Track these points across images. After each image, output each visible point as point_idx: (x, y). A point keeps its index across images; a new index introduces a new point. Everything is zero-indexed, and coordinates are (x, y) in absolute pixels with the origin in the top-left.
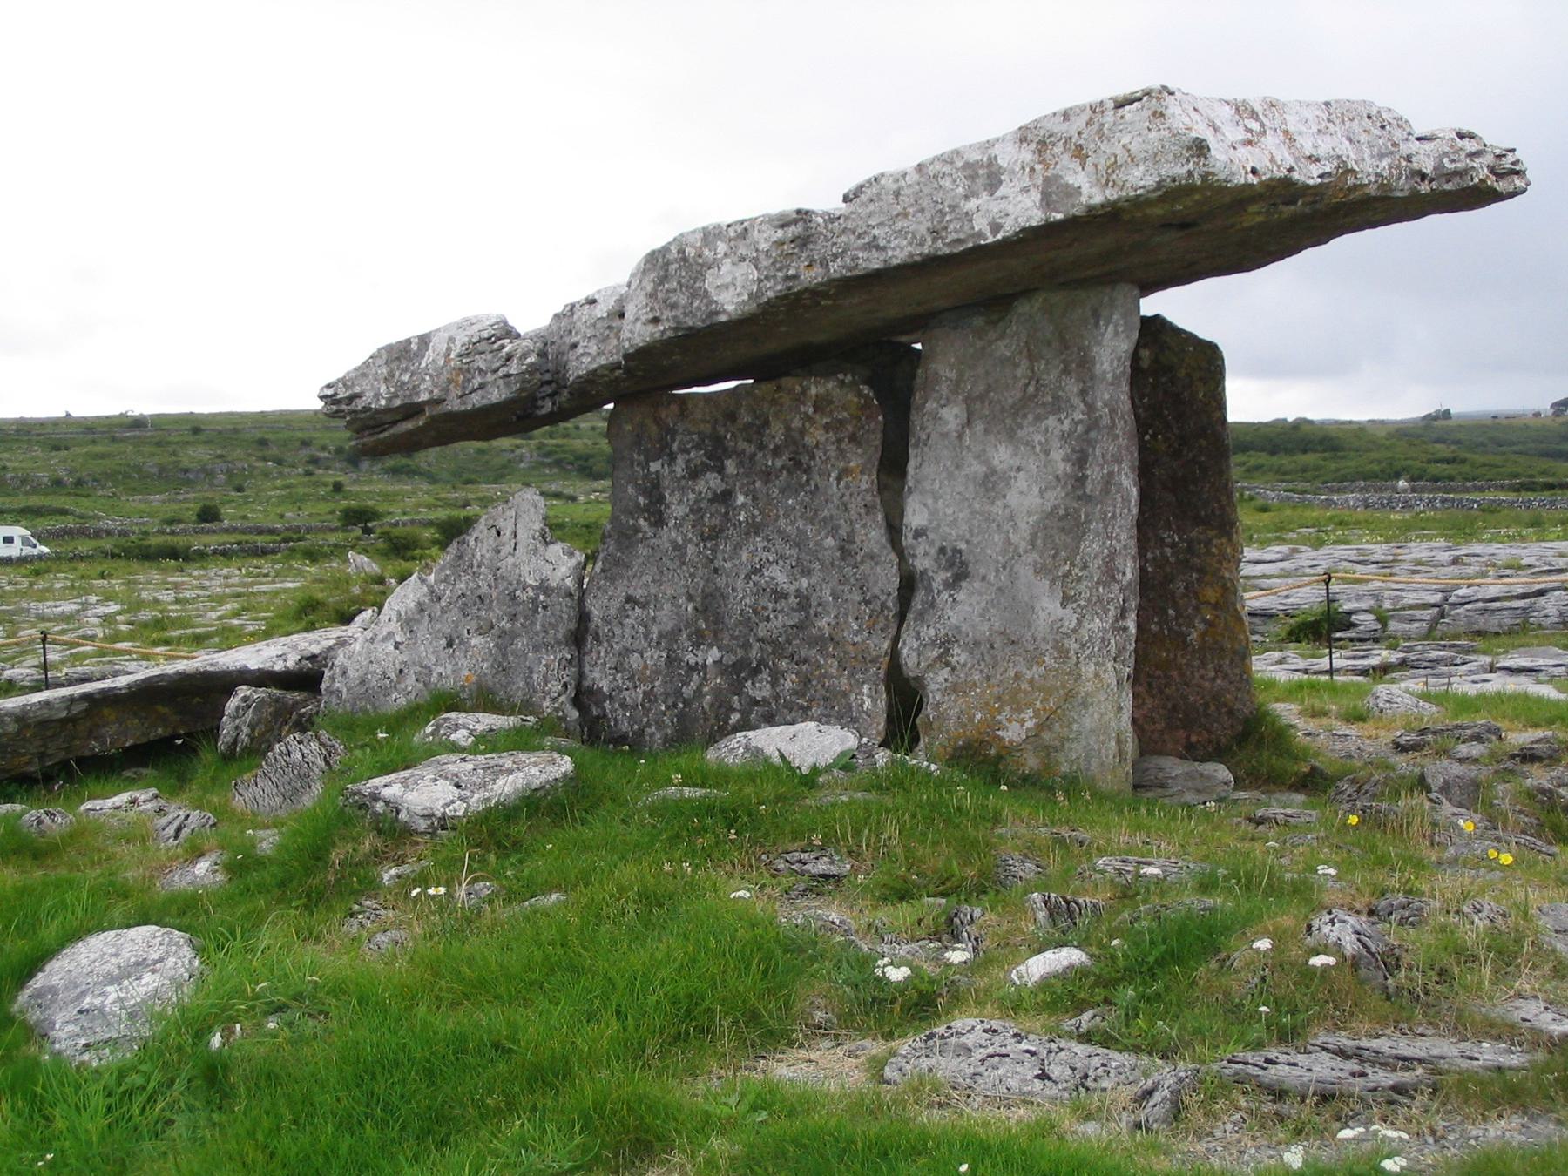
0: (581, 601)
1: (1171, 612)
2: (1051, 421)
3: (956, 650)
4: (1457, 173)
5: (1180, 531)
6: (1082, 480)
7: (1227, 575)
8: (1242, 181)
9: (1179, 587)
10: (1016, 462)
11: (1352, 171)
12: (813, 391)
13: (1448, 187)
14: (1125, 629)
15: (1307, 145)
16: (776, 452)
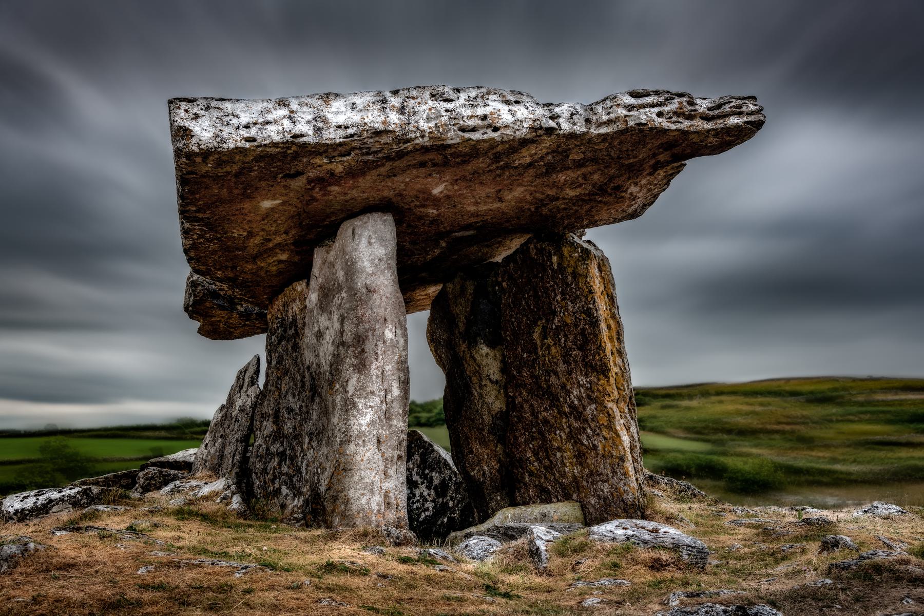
0: (252, 419)
1: (589, 431)
2: (336, 299)
3: (314, 439)
4: (610, 122)
5: (586, 375)
6: (342, 333)
7: (610, 405)
8: (232, 146)
9: (588, 411)
10: (327, 323)
11: (386, 132)
12: (299, 289)
13: (603, 130)
14: (391, 426)
15: (341, 120)
16: (290, 329)
